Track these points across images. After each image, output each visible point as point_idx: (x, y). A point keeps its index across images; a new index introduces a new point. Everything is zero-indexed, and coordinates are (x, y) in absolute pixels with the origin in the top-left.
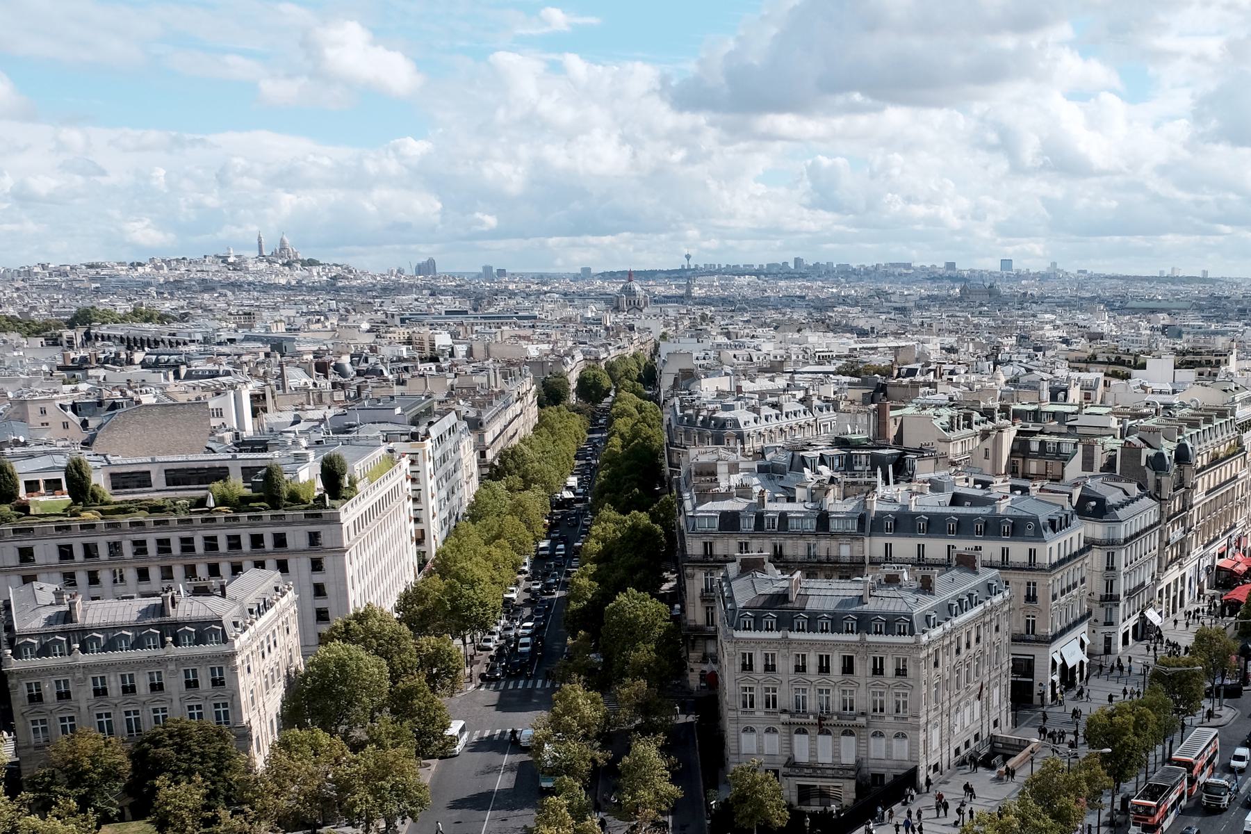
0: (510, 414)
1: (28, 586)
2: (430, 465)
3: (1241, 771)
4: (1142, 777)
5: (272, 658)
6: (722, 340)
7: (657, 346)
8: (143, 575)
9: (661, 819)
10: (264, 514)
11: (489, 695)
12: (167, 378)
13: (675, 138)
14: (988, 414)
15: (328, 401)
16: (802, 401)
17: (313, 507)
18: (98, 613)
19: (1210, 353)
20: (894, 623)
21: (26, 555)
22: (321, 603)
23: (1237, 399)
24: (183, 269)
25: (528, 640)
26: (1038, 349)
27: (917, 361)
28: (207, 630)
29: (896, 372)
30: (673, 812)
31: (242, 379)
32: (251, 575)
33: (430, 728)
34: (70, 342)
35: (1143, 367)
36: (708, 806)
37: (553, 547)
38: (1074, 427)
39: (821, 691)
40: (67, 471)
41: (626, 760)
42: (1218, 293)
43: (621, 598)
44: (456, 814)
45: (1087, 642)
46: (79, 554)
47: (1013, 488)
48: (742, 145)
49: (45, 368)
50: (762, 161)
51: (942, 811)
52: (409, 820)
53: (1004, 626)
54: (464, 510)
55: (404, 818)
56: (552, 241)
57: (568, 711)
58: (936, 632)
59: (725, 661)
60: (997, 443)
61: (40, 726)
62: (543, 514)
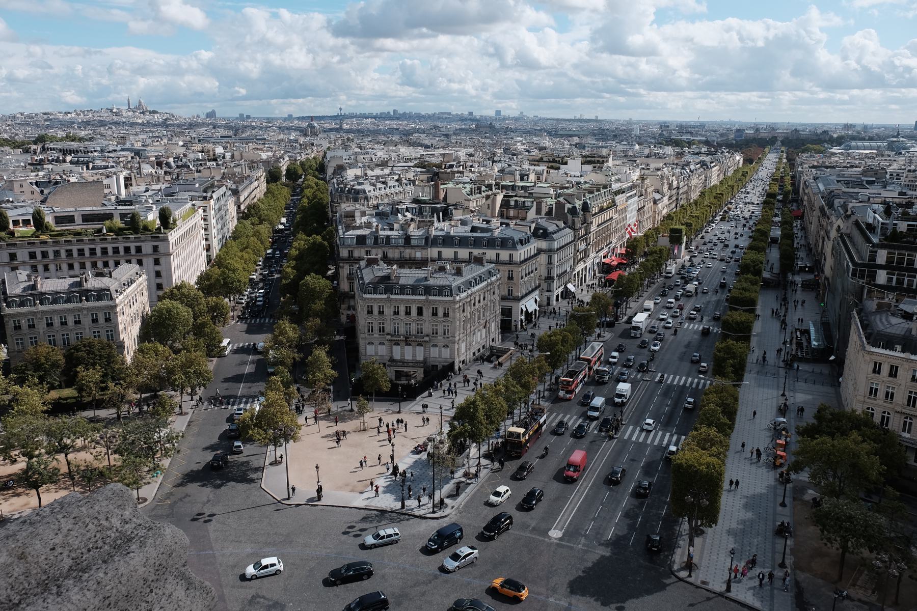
0: (252, 187)
1: (14, 272)
2: (213, 212)
3: (615, 363)
4: (565, 367)
5: (135, 308)
6: (358, 150)
7: (325, 153)
8: (71, 266)
9: (327, 387)
10: (131, 236)
11: (242, 326)
12: (82, 169)
13: (335, 50)
14: (489, 187)
15: (162, 180)
16: (397, 181)
17: (155, 233)
18: (49, 285)
19: (599, 157)
20: (442, 290)
21: (13, 257)
22: (159, 281)
23: (613, 180)
24: (91, 115)
25: (261, 299)
26: (514, 155)
27: (454, 160)
28: (103, 294)
29: (443, 166)
30: (333, 384)
31: (120, 169)
32: (124, 267)
33: (213, 342)
34: (35, 151)
35: (566, 163)
36: (351, 381)
37: (274, 253)
38: (532, 193)
39: (406, 324)
40: (33, 215)
41: (310, 358)
42: (603, 127)
43: (308, 278)
44: (226, 385)
45: (538, 300)
46: (39, 256)
47: (502, 224)
48: (367, 54)
49: (22, 164)
50: (378, 62)
51: (466, 384)
52: (202, 388)
53: (497, 292)
54: (230, 234)
55: (200, 387)
56: (274, 101)
57: (281, 334)
58: (464, 295)
59: (359, 309)
60: (494, 201)
61: (20, 341)
62: (269, 237)
